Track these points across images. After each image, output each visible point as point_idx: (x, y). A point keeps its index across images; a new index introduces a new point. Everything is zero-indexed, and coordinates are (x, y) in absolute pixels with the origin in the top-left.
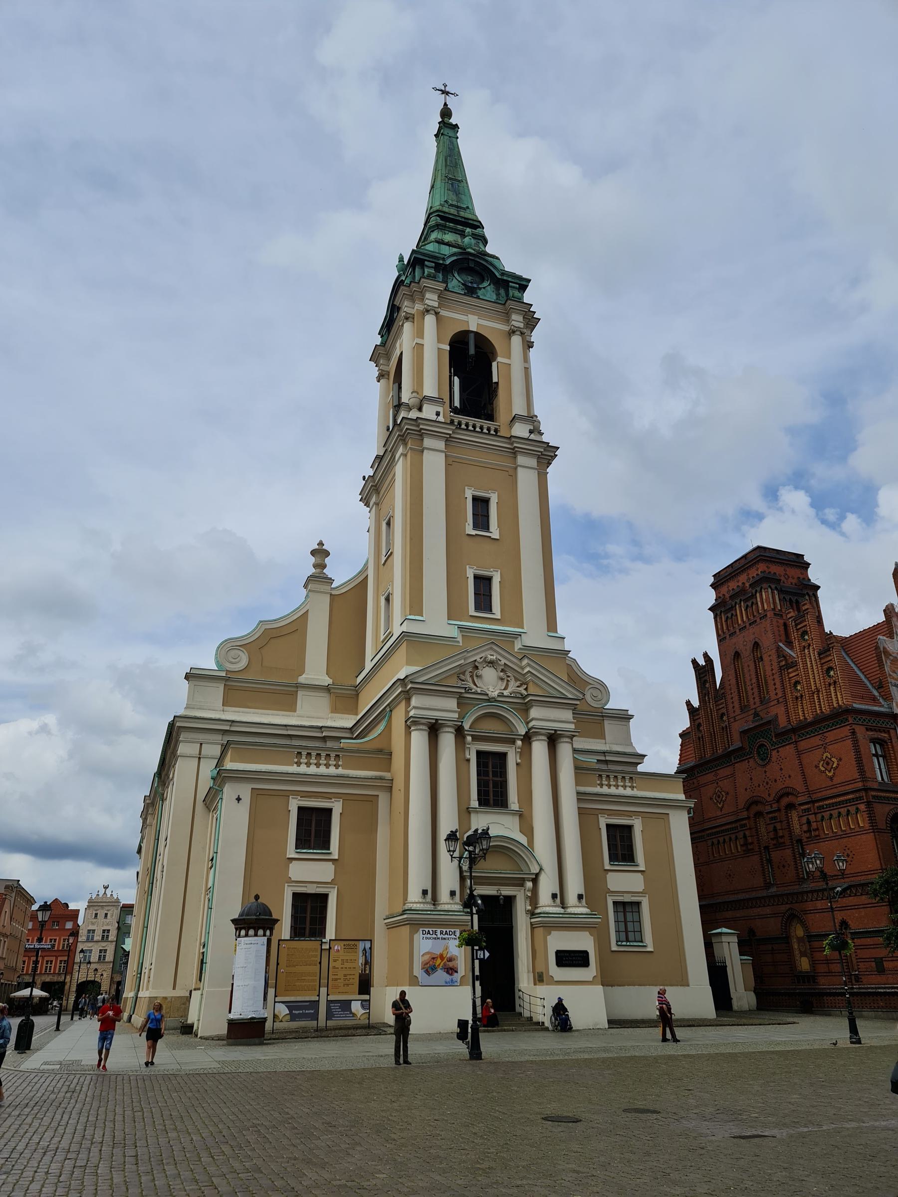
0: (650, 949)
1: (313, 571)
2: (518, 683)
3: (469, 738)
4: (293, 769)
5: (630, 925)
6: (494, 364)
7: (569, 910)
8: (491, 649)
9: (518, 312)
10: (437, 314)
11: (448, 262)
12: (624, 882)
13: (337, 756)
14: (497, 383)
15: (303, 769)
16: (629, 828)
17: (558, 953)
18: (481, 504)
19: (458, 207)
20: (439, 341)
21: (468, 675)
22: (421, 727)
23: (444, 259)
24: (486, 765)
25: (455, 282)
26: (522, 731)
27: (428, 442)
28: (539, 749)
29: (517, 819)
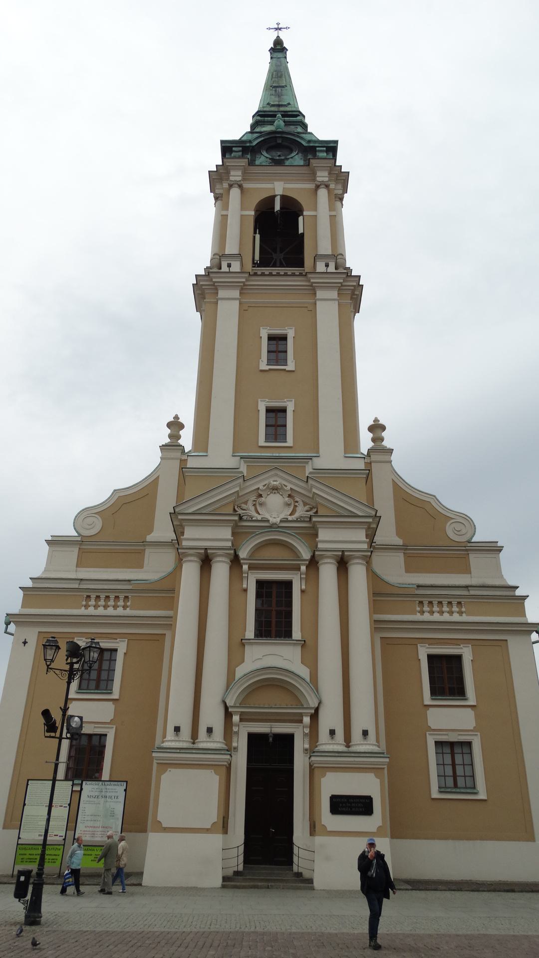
0: (482, 796)
1: (167, 440)
2: (307, 507)
3: (245, 567)
4: (82, 611)
5: (460, 770)
6: (301, 219)
7: (352, 749)
8: (276, 475)
9: (323, 168)
10: (240, 186)
11: (254, 143)
12: (450, 719)
13: (126, 597)
14: (303, 234)
15: (91, 611)
16: (458, 658)
17: (333, 798)
18: (277, 341)
19: (279, 106)
20: (243, 208)
21: (250, 504)
22: (189, 558)
23: (250, 142)
24: (269, 595)
25: (263, 158)
26: (306, 555)
27: (222, 293)
28: (328, 572)
29: (298, 649)
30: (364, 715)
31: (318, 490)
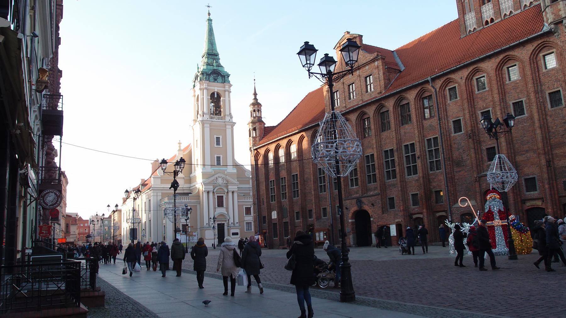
18: (218, 139)
30: (237, 220)
31: (228, 178)
